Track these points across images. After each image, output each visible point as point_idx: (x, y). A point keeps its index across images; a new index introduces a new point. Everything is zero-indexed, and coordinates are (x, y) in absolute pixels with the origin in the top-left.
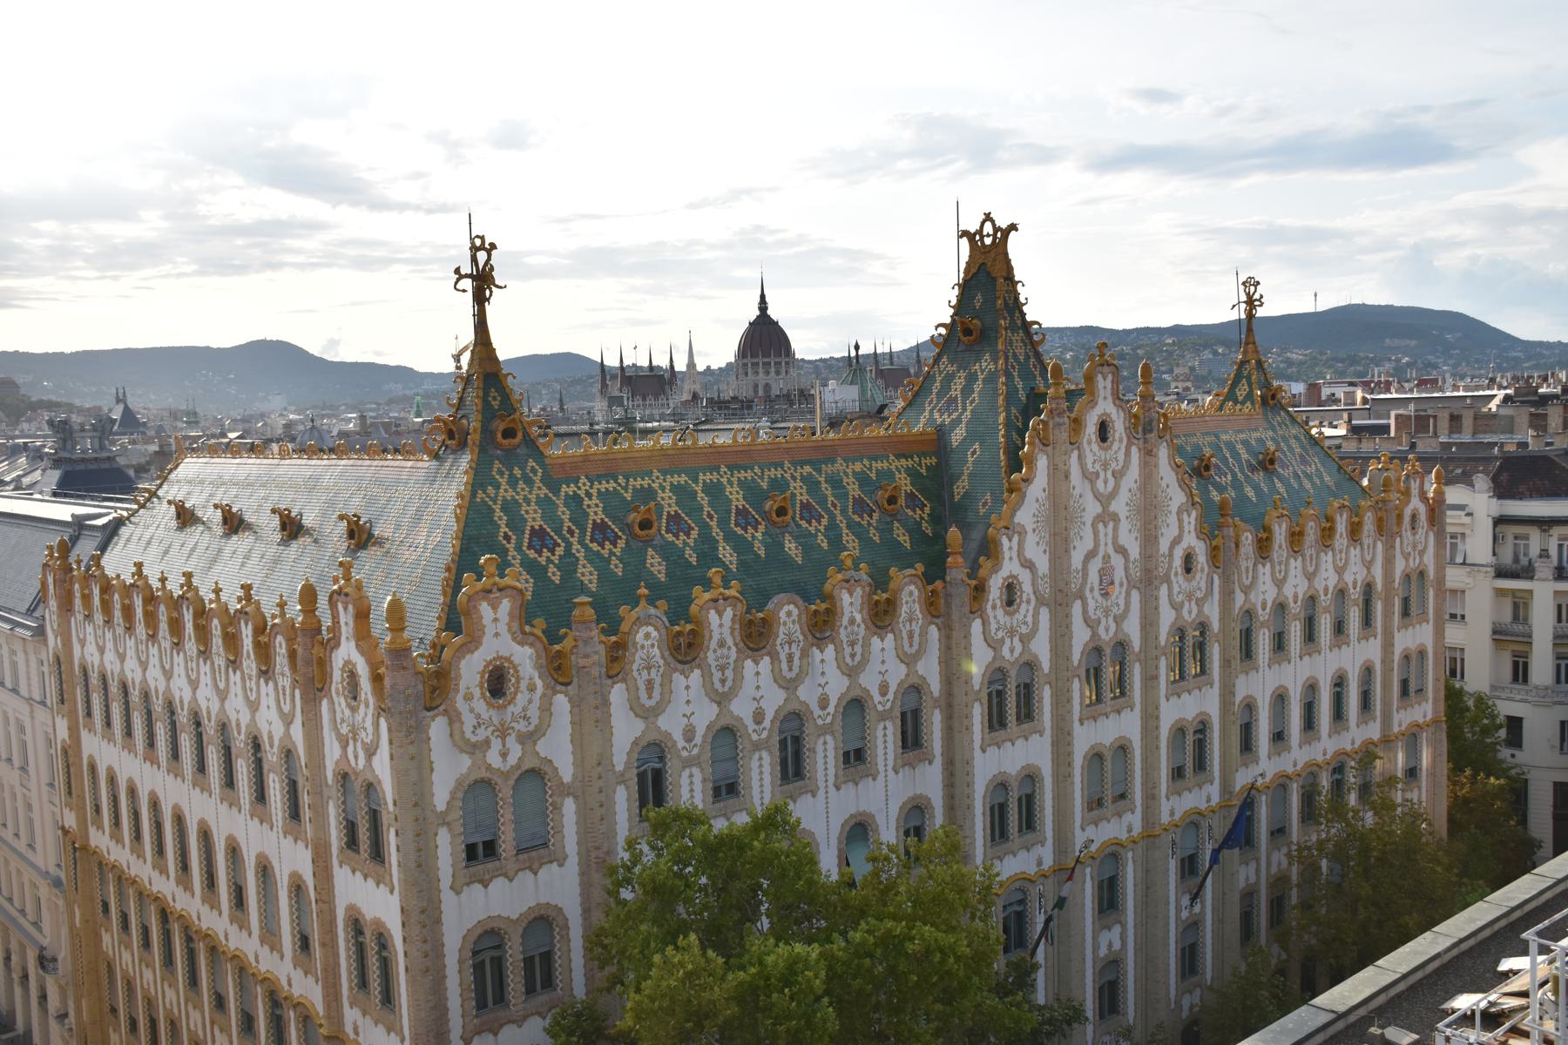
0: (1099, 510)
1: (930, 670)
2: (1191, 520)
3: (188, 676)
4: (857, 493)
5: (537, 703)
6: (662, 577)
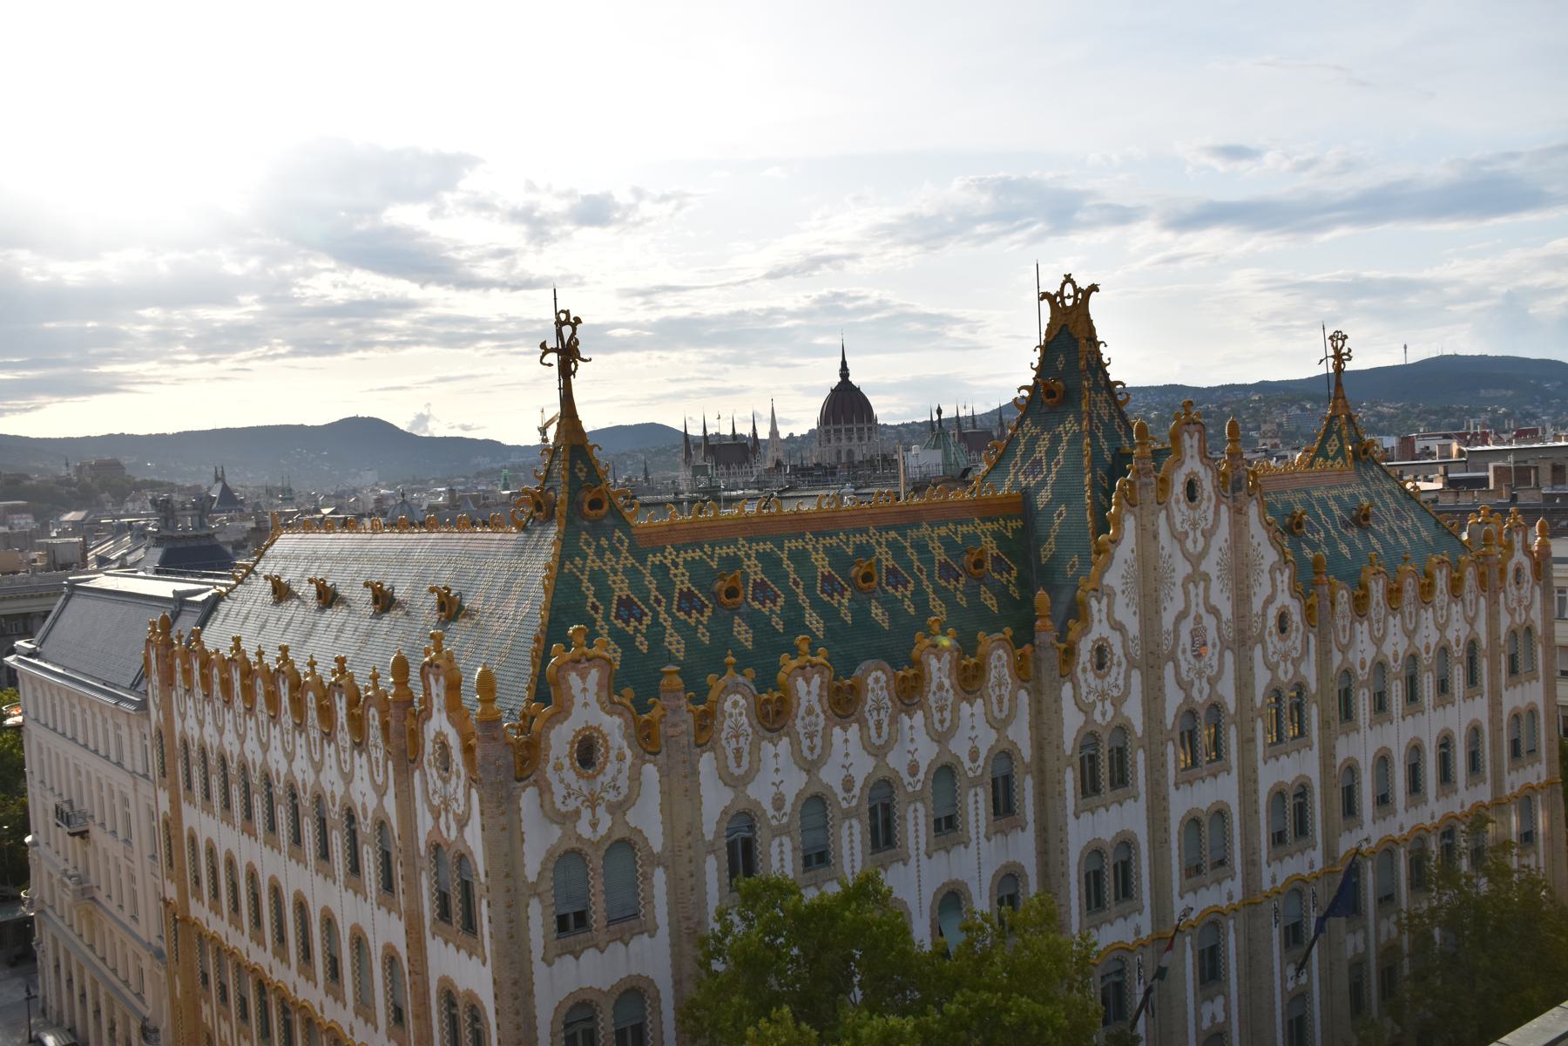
0: (1189, 569)
1: (1021, 735)
2: (1284, 578)
3: (284, 749)
4: (943, 557)
5: (626, 772)
6: (749, 645)
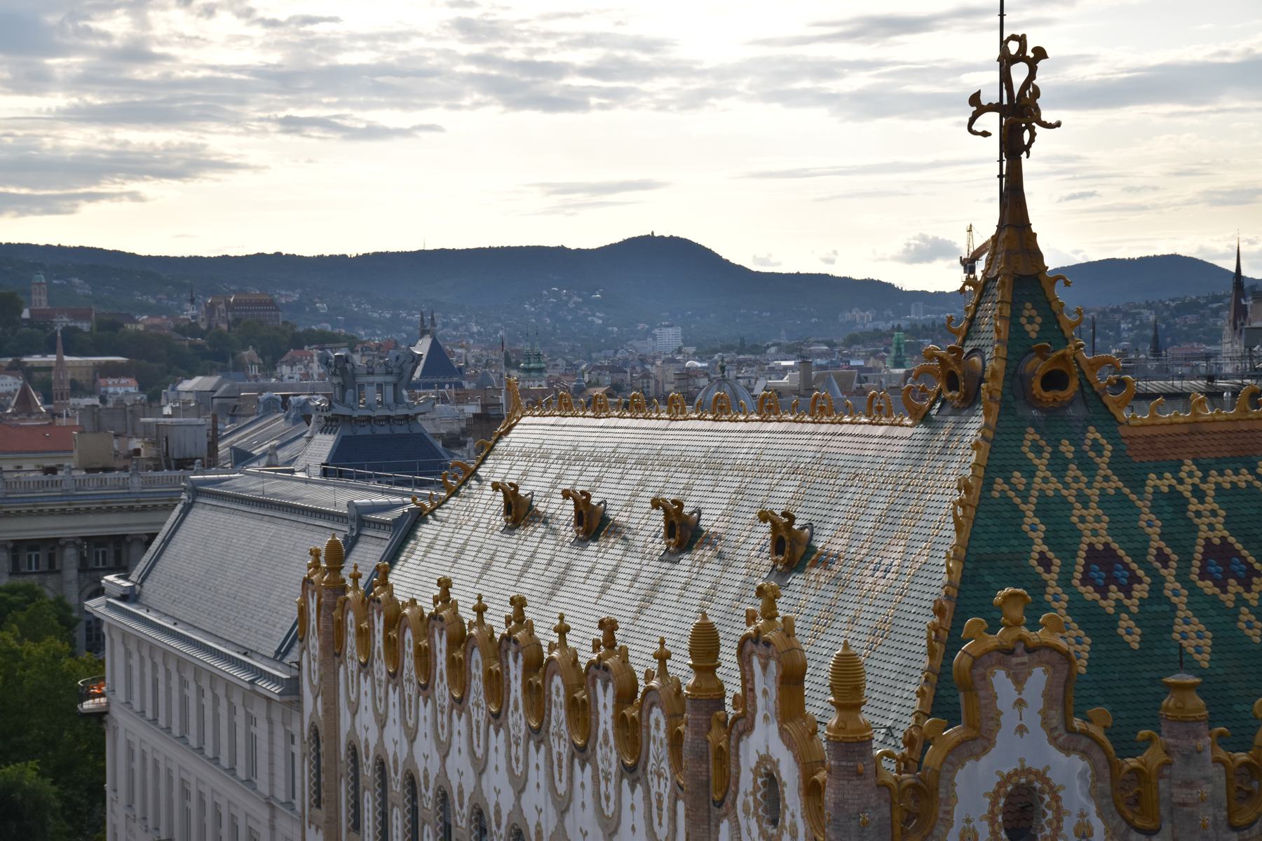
3: (510, 770)
